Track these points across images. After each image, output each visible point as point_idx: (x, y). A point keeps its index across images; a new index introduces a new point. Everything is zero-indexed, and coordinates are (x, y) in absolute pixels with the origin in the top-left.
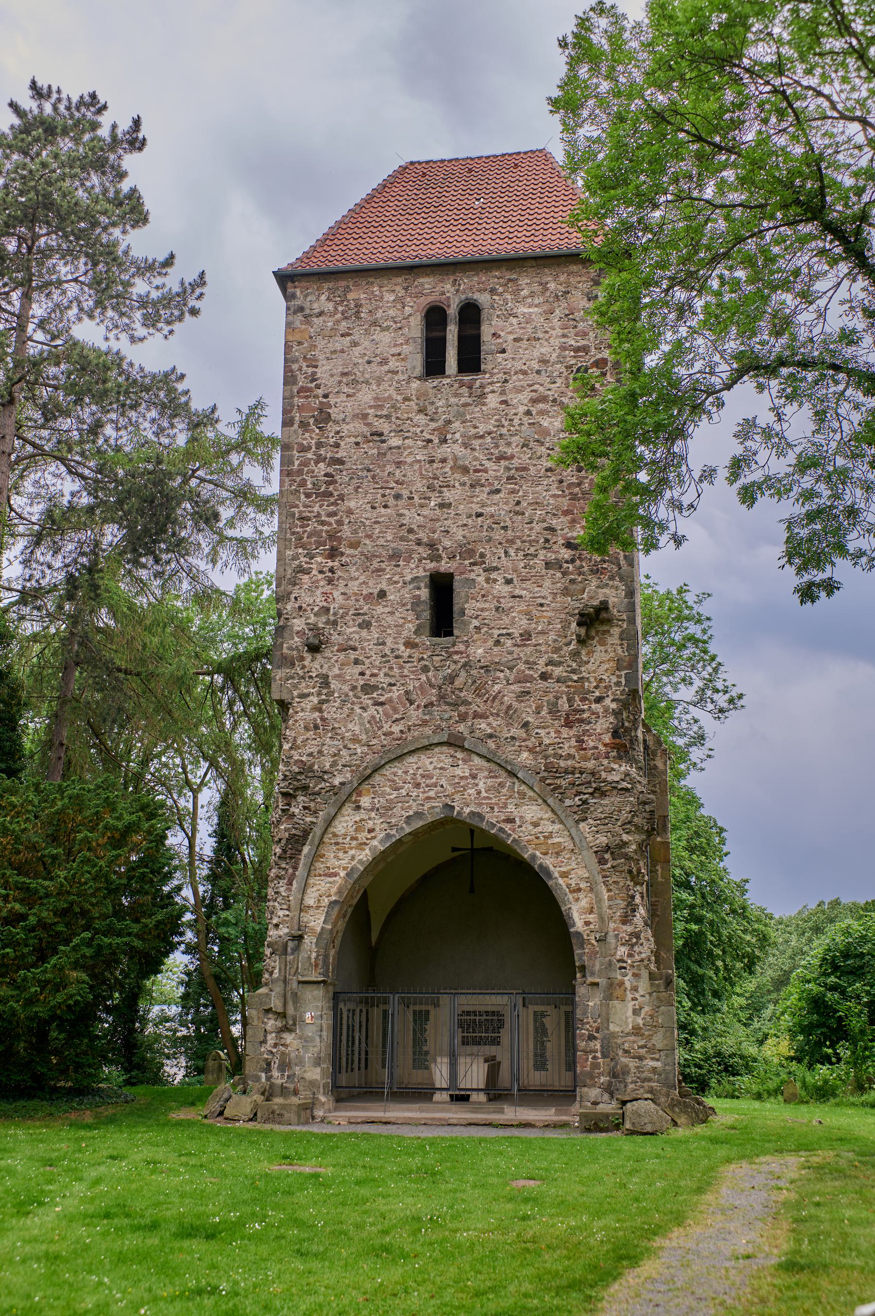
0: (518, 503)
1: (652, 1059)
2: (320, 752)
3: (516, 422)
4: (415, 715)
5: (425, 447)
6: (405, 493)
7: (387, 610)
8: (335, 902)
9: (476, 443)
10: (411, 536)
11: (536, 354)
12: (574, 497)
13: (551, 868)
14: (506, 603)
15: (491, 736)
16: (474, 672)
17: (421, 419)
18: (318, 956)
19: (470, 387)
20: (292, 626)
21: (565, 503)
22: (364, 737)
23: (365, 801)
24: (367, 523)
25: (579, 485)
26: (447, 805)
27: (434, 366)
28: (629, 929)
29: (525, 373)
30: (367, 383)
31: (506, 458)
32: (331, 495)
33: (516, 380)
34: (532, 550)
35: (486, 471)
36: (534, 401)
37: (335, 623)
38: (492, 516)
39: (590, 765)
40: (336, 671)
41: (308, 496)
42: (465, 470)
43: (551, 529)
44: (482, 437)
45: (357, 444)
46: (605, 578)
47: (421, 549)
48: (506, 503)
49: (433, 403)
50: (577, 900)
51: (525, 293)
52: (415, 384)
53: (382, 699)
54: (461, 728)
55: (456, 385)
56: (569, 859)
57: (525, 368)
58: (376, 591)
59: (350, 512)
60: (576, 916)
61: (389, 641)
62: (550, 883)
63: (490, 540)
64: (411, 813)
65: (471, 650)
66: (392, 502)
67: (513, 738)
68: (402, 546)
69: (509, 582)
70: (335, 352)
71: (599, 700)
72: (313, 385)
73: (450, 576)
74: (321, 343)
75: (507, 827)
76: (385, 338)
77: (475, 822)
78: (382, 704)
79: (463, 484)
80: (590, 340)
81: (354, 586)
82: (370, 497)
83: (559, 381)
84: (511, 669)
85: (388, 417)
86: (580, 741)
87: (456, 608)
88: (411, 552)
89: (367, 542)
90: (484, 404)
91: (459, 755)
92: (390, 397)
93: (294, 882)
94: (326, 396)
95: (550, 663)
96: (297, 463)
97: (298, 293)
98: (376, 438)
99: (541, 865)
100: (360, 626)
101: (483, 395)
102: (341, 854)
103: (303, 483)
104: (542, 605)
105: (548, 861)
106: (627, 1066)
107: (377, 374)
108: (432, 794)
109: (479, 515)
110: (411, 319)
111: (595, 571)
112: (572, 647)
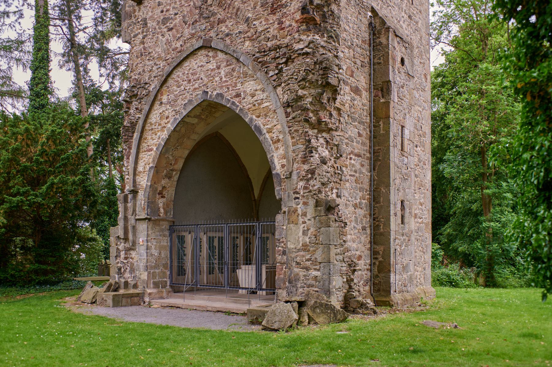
1: (315, 269)
2: (144, 71)
4: (187, 32)
8: (152, 167)
13: (262, 126)
15: (227, 35)
18: (145, 202)
22: (163, 55)
23: (165, 99)
26: (204, 91)
28: (306, 167)
40: (150, 14)
50: (277, 149)
53: (172, 26)
56: (272, 118)
60: (276, 161)
62: (261, 138)
64: (186, 102)
75: (236, 100)
77: (219, 101)
86: (281, 23)
91: (211, 54)
93: (130, 157)
99: (256, 126)
102: (154, 136)
105: (260, 122)
106: (298, 274)
108: (196, 86)
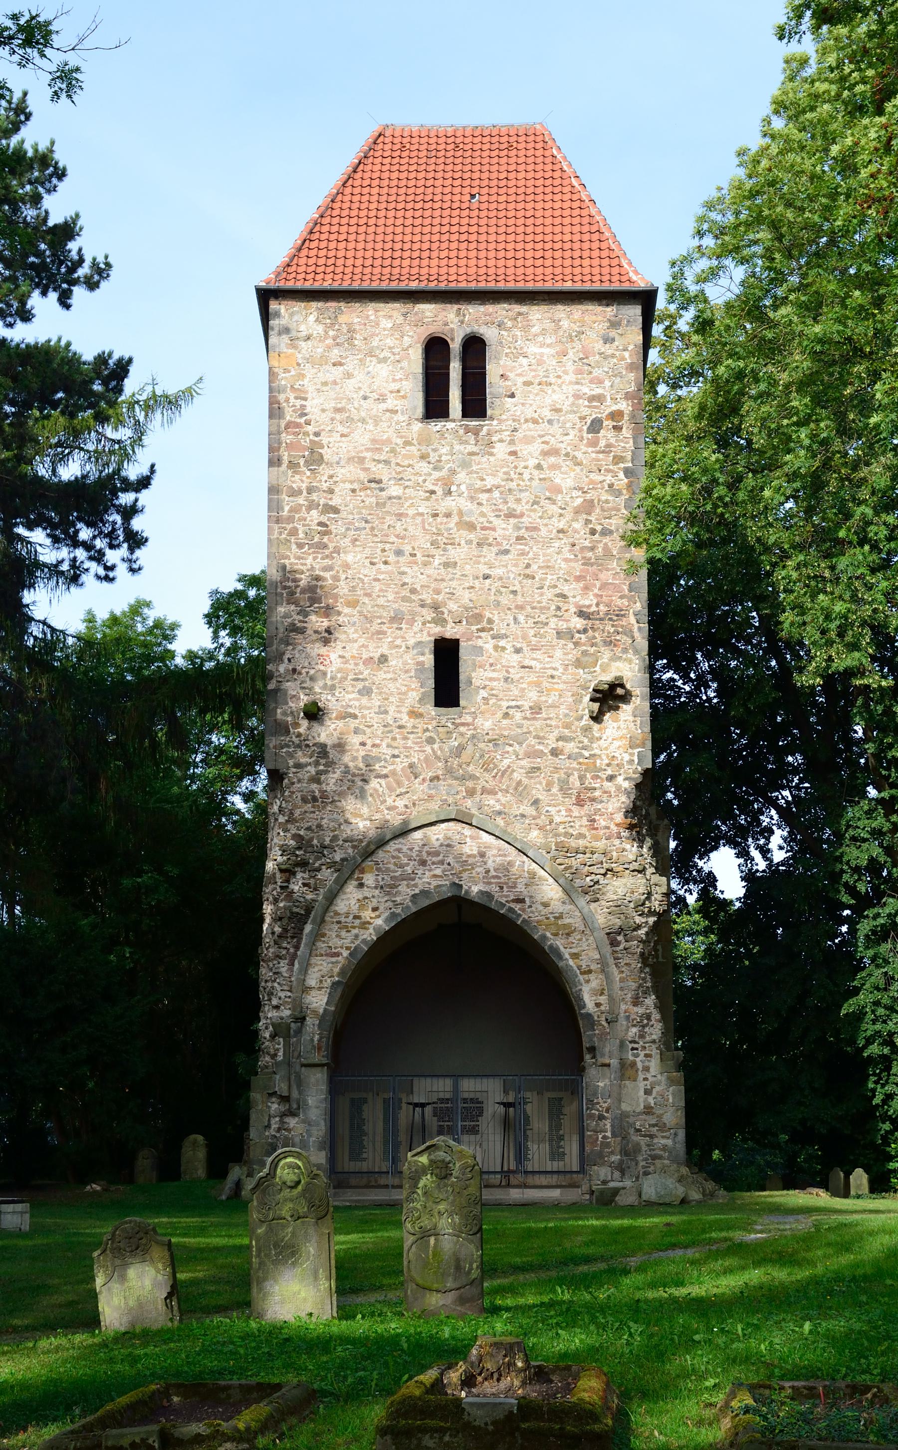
0: (528, 566)
3: (526, 476)
5: (427, 499)
6: (407, 549)
7: (389, 676)
9: (484, 497)
10: (413, 597)
11: (548, 401)
12: (587, 563)
14: (515, 674)
15: (500, 813)
16: (482, 745)
17: (423, 467)
19: (476, 434)
20: (286, 691)
21: (578, 568)
24: (366, 579)
25: (592, 549)
27: (435, 408)
29: (535, 422)
30: (363, 421)
31: (515, 516)
32: (325, 546)
33: (526, 429)
34: (543, 618)
35: (494, 529)
36: (545, 454)
37: (333, 688)
38: (501, 579)
39: (600, 845)
41: (300, 546)
42: (471, 527)
43: (563, 596)
44: (489, 491)
45: (354, 491)
46: (618, 651)
47: (424, 611)
48: (516, 565)
49: (435, 450)
51: (535, 330)
52: (417, 426)
53: (385, 771)
54: (469, 803)
55: (461, 432)
57: (536, 416)
58: (377, 656)
59: (347, 566)
61: (392, 709)
63: (498, 604)
65: (479, 721)
66: (392, 558)
67: (523, 816)
68: (405, 607)
69: (518, 651)
70: (325, 384)
71: (611, 778)
72: (302, 420)
73: (456, 642)
74: (309, 371)
75: (517, 907)
76: (383, 371)
78: (386, 776)
79: (469, 542)
80: (604, 389)
81: (353, 649)
82: (368, 551)
83: (572, 433)
84: (520, 744)
85: (387, 462)
87: (462, 677)
88: (414, 614)
89: (366, 600)
90: (492, 454)
92: (388, 441)
94: (317, 434)
95: (560, 739)
96: (287, 508)
97: (283, 311)
98: (373, 485)
100: (359, 692)
101: (490, 444)
103: (294, 532)
104: (552, 677)
107: (374, 412)
109: (486, 577)
110: (411, 351)
111: (608, 643)
112: (583, 723)
